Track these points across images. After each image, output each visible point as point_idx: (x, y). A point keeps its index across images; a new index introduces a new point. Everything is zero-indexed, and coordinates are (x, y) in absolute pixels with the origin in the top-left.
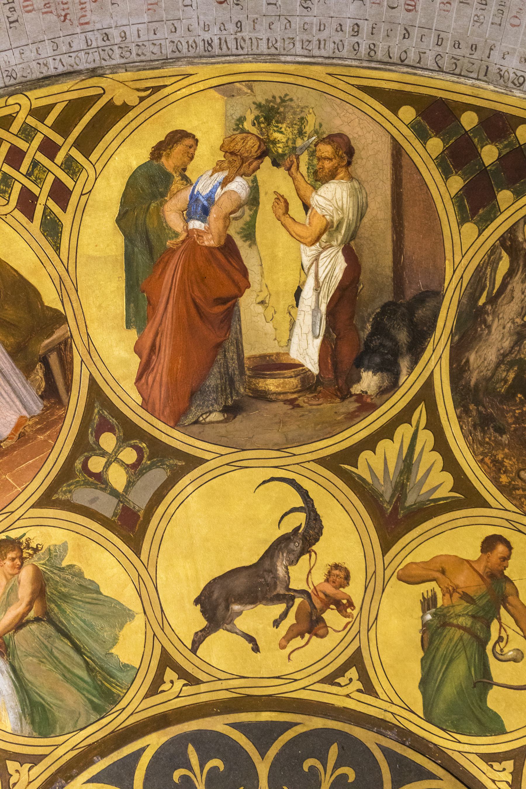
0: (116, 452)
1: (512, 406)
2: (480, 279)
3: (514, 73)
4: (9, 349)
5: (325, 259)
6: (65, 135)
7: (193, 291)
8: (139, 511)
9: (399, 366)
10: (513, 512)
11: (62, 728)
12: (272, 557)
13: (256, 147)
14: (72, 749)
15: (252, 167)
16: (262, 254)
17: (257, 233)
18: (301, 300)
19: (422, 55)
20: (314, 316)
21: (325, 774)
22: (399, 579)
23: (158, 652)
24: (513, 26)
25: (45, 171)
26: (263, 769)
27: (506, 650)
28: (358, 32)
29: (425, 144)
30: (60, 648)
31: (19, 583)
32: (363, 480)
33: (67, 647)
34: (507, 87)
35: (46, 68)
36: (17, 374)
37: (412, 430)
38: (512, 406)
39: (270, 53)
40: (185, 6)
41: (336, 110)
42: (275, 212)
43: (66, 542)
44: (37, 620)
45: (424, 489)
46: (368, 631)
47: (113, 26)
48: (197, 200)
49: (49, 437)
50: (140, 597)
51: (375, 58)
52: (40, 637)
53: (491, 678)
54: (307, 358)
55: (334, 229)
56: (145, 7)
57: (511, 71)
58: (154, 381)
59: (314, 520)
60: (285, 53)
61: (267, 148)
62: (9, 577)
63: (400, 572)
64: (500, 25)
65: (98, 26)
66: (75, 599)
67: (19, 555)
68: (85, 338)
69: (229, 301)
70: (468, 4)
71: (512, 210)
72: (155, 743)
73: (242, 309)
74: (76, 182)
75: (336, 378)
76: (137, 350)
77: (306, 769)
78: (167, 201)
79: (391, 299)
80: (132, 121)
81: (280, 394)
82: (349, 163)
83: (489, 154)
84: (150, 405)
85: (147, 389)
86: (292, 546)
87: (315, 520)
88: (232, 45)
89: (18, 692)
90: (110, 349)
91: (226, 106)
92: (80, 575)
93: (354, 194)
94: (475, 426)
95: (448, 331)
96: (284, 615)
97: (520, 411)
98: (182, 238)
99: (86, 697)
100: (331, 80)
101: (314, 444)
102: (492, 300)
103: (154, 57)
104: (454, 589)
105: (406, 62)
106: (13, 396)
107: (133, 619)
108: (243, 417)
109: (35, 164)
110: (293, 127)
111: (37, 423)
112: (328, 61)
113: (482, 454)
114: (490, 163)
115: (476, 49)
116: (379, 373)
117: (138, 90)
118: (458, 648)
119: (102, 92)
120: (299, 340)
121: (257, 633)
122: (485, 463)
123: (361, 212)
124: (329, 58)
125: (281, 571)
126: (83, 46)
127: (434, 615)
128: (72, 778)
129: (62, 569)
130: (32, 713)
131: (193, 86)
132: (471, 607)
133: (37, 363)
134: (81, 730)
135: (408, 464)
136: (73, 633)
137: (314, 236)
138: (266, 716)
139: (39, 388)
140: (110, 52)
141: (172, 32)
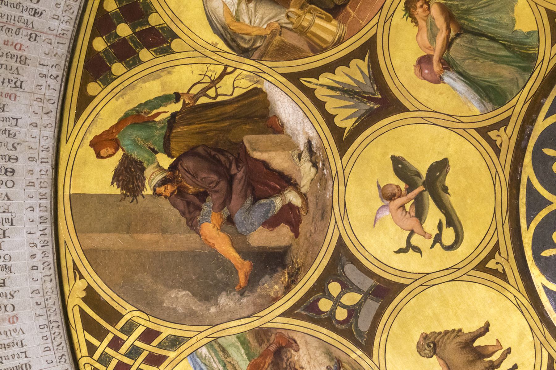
11: (511, 94)
31: (434, 18)
33: (486, 42)
44: (458, 35)
52: (466, 45)
62: (425, 18)
66: (474, 9)
89: (471, 87)
99: (515, 66)
128: (534, 121)
134: (524, 88)
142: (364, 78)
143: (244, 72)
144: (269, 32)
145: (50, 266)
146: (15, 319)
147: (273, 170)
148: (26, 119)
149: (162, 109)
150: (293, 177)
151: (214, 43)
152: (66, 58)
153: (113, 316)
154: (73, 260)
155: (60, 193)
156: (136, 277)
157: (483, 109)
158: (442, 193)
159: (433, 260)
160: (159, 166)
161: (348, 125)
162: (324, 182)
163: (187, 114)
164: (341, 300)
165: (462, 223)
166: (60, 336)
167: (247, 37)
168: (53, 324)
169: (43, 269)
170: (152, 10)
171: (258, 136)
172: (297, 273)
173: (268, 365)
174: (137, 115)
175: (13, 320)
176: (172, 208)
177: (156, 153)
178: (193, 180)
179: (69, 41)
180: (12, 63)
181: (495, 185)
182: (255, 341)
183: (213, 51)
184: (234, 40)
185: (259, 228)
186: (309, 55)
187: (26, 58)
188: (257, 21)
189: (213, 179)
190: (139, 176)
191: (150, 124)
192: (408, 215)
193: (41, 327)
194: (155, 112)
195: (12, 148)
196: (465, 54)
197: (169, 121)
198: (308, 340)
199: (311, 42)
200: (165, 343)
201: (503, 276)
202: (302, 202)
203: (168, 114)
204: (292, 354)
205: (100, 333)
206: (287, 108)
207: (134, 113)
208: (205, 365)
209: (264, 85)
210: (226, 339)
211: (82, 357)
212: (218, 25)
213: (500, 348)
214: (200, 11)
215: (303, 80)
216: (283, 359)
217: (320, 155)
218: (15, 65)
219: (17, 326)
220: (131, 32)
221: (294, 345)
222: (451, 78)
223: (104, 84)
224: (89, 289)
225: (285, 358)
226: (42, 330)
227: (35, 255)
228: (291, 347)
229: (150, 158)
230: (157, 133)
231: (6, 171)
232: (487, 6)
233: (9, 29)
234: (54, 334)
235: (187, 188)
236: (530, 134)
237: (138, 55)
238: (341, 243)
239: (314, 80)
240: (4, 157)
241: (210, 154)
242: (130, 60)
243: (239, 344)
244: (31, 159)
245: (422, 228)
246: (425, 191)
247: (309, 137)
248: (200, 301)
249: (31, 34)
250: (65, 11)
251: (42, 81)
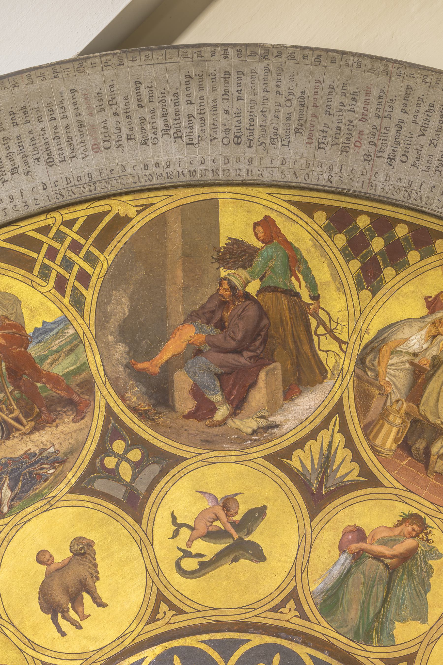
11: (332, 621)
14: (323, 634)
23: (413, 650)
30: (379, 591)
31: (402, 542)
44: (387, 566)
50: (439, 620)
52: (378, 574)
62: (402, 534)
66: (413, 581)
67: (418, 532)
89: (337, 581)
92: (430, 575)
107: (423, 623)
128: (306, 645)
129: (426, 563)
130: (330, 597)
134: (338, 633)
142: (341, 477)
143: (342, 361)
144: (382, 383)
145: (148, 181)
146: (96, 150)
147: (248, 391)
148: (289, 154)
149: (303, 283)
150: (243, 411)
151: (369, 331)
152: (349, 190)
153: (102, 243)
154: (155, 204)
155: (220, 189)
156: (141, 264)
157: (316, 593)
158: (232, 557)
159: (165, 548)
160: (248, 282)
161: (295, 463)
162: (238, 441)
163: (299, 308)
164: (124, 463)
165: (203, 577)
166: (81, 193)
167: (376, 363)
168: (93, 186)
169: (145, 175)
170: (398, 271)
171: (281, 375)
172: (149, 419)
173: (58, 394)
174: (296, 259)
175: (96, 148)
176: (208, 297)
177: (261, 279)
178: (236, 316)
179: (366, 191)
180: (342, 140)
181: (242, 608)
182: (82, 380)
183: (361, 330)
184: (372, 349)
185: (191, 380)
186: (362, 422)
187: (347, 152)
188: (392, 371)
189: (237, 335)
190: (238, 264)
191: (288, 272)
192: (209, 524)
193: (90, 175)
194: (300, 277)
195: (261, 142)
196: (369, 573)
197: (292, 290)
198: (84, 431)
199: (374, 424)
200: (77, 294)
201: (152, 619)
202: (218, 421)
203: (298, 290)
204: (70, 416)
205: (85, 231)
206: (309, 404)
207: (299, 257)
208: (57, 333)
209: (331, 381)
210: (83, 352)
211: (62, 215)
212: (387, 334)
213: (82, 618)
214: (400, 316)
215: (336, 418)
216: (65, 408)
217: (265, 437)
218: (340, 142)
219: (90, 152)
220: (376, 252)
221: (79, 418)
222: (345, 561)
223: (325, 227)
224: (127, 219)
225: (66, 409)
226: (86, 176)
227: (159, 167)
228: (77, 415)
229: (255, 274)
230: (280, 280)
231: (238, 137)
232: (417, 594)
233: (375, 135)
234: (83, 187)
235: (227, 311)
236: (293, 641)
237: (354, 259)
238: (180, 460)
239: (337, 428)
240: (251, 134)
241: (261, 330)
242: (349, 251)
243: (78, 365)
244: (250, 160)
245: (198, 539)
246: (234, 540)
247: (282, 425)
248: (119, 326)
249: (371, 156)
250: (394, 187)
251: (325, 168)
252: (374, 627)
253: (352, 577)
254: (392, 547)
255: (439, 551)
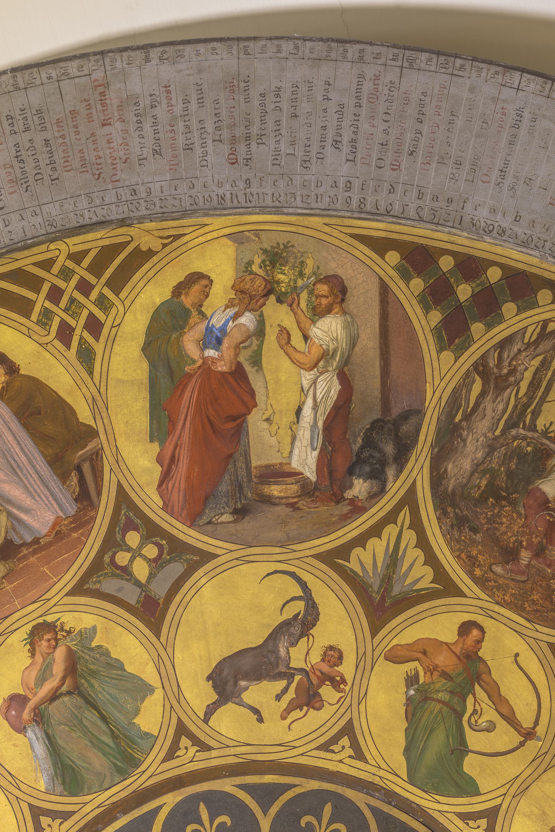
0: (140, 548)
1: (486, 508)
2: (457, 399)
3: (485, 222)
4: (48, 459)
5: (322, 382)
6: (99, 276)
7: (207, 409)
8: (159, 599)
9: (386, 474)
10: (486, 601)
11: (90, 788)
12: (275, 639)
13: (263, 286)
14: (98, 807)
15: (258, 304)
16: (268, 378)
17: (263, 360)
18: (301, 417)
19: (405, 207)
20: (312, 432)
21: (320, 829)
22: (386, 659)
23: (174, 722)
24: (484, 182)
25: (81, 307)
26: (265, 824)
27: (480, 721)
28: (350, 188)
29: (409, 283)
30: (89, 718)
31: (54, 661)
32: (355, 573)
34: (479, 234)
35: (82, 218)
36: (54, 480)
37: (399, 529)
38: (484, 508)
39: (275, 206)
40: (202, 166)
41: (331, 255)
42: (279, 342)
43: (95, 626)
44: (69, 693)
45: (408, 581)
46: (359, 704)
47: (140, 183)
48: (212, 332)
49: (82, 534)
50: (160, 673)
51: (364, 210)
52: (72, 708)
53: (467, 746)
54: (306, 468)
55: (329, 356)
56: (167, 168)
57: (482, 220)
58: (173, 487)
59: (312, 607)
60: (287, 205)
61: (272, 288)
62: (45, 655)
63: (387, 653)
64: (472, 181)
65: (127, 183)
66: (103, 675)
67: (54, 636)
68: (114, 450)
69: (238, 419)
70: (445, 164)
71: (484, 340)
72: (171, 802)
73: (249, 425)
74: (107, 316)
75: (331, 484)
76: (159, 460)
77: (303, 824)
78: (185, 333)
79: (379, 417)
80: (156, 264)
81: (282, 498)
82: (343, 300)
83: (464, 292)
84: (170, 508)
85: (167, 493)
86: (292, 630)
87: (313, 607)
88: (242, 199)
89: (51, 756)
90: (136, 460)
91: (237, 251)
92: (107, 654)
93: (347, 326)
94: (452, 526)
95: (428, 444)
96: (285, 690)
97: (491, 513)
98: (198, 364)
99: (110, 761)
100: (327, 229)
101: (312, 542)
102: (467, 417)
103: (174, 209)
104: (434, 668)
105: (391, 213)
106: (51, 499)
107: (153, 693)
108: (251, 518)
109: (72, 300)
110: (294, 270)
111: (71, 523)
112: (324, 213)
113: (458, 551)
114: (465, 299)
115: (451, 202)
116: (369, 480)
117: (161, 238)
118: (438, 719)
119: (131, 239)
120: (300, 452)
121: (261, 706)
122: (461, 558)
123: (353, 342)
124: (325, 209)
125: (282, 652)
126: (114, 200)
127: (417, 690)
131: (208, 234)
132: (449, 684)
133: (72, 471)
134: (106, 790)
135: (394, 559)
136: (100, 704)
137: (313, 363)
138: (268, 779)
139: (74, 492)
140: (137, 205)
141: (190, 188)
157: (50, 788)
196: (65, 717)
222: (35, 734)
232: (119, 679)
252: (125, 748)
253: (57, 738)
254: (52, 675)
255: (88, 627)
